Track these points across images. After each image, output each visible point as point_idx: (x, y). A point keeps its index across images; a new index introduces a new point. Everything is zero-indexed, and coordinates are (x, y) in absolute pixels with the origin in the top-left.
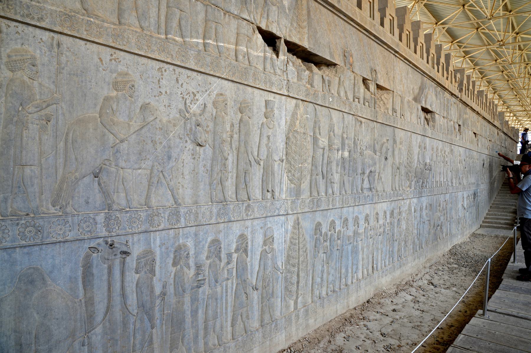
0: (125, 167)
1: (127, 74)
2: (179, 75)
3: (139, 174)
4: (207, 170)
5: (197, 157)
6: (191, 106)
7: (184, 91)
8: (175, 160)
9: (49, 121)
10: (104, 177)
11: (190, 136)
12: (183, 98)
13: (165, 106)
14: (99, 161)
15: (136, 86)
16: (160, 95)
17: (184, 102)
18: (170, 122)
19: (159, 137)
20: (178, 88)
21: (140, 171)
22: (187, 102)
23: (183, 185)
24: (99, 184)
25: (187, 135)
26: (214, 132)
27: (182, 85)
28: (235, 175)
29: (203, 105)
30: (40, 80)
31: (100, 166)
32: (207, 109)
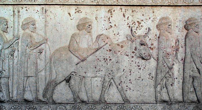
0: (86, 76)
1: (86, 18)
2: (125, 12)
3: (96, 80)
4: (152, 77)
5: (142, 68)
6: (136, 32)
7: (130, 22)
8: (123, 71)
9: (42, 53)
10: (72, 82)
11: (135, 53)
12: (129, 27)
13: (115, 34)
14: (69, 73)
15: (92, 25)
16: (111, 28)
17: (130, 29)
18: (118, 45)
19: (109, 56)
20: (125, 21)
21: (96, 79)
22: (133, 29)
23: (130, 88)
24: (69, 87)
25: (133, 52)
26: (158, 48)
27: (128, 18)
28: (181, 81)
29: (148, 29)
30: (37, 32)
31: (69, 76)
32: (151, 32)
